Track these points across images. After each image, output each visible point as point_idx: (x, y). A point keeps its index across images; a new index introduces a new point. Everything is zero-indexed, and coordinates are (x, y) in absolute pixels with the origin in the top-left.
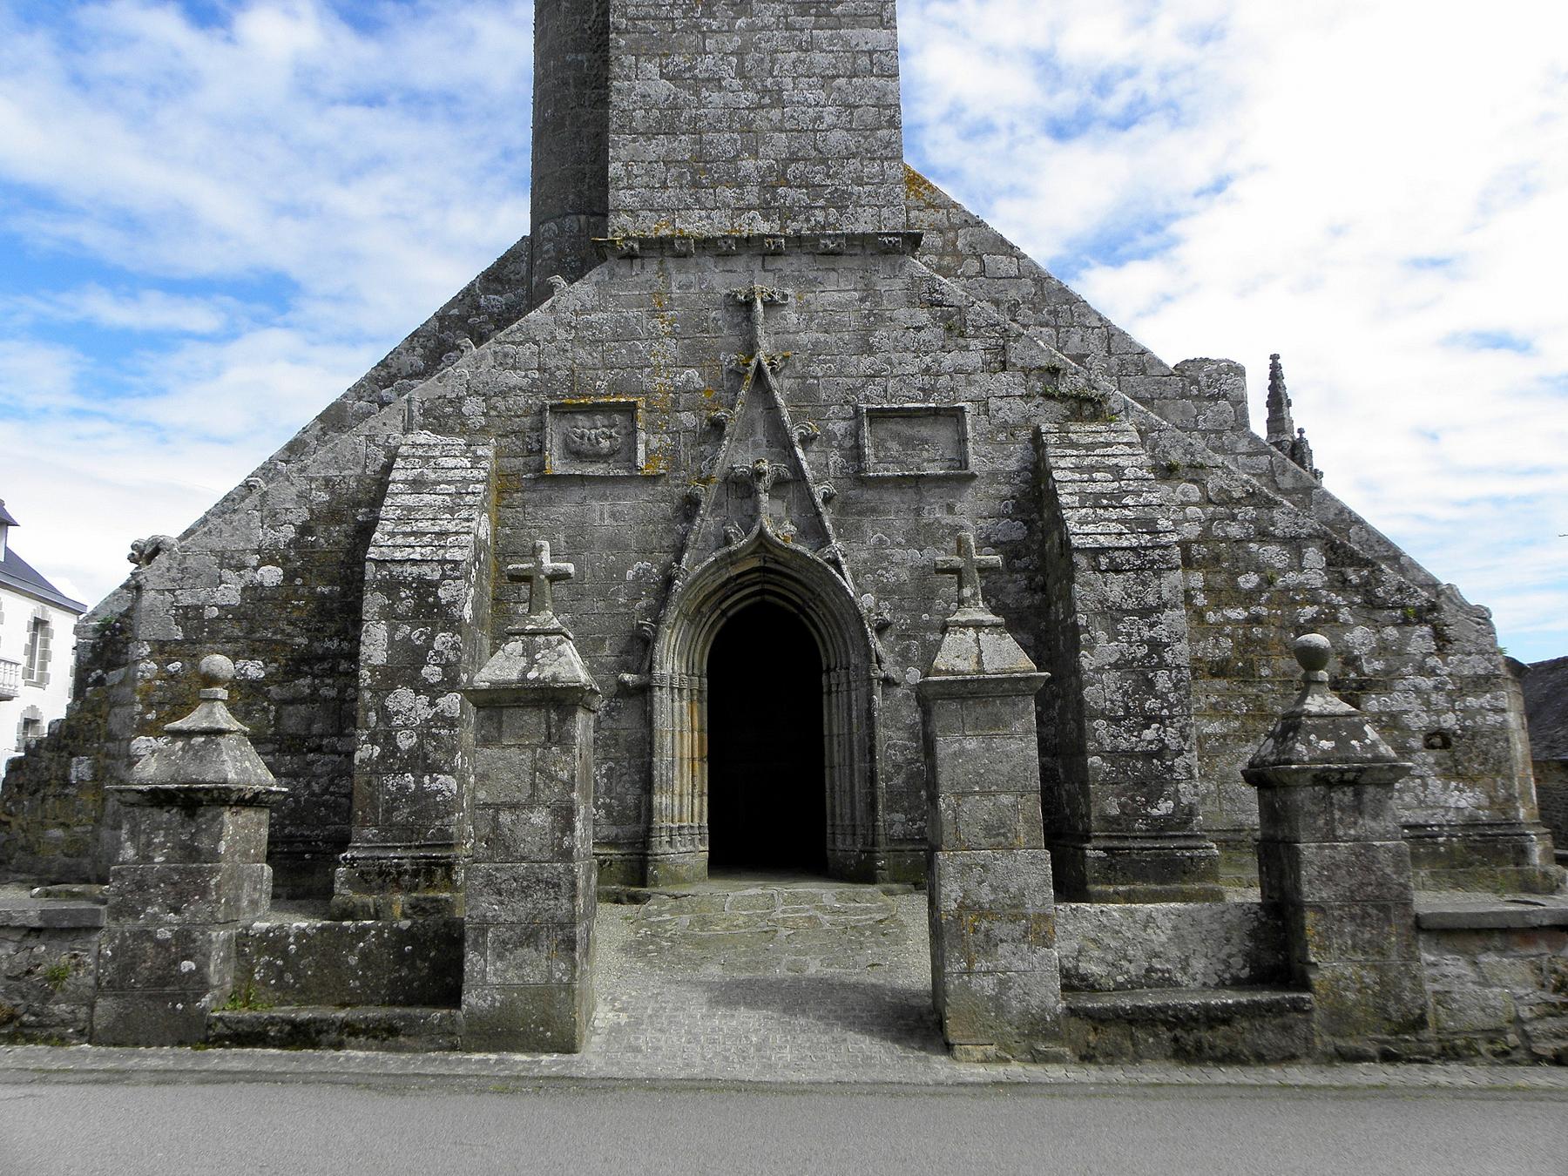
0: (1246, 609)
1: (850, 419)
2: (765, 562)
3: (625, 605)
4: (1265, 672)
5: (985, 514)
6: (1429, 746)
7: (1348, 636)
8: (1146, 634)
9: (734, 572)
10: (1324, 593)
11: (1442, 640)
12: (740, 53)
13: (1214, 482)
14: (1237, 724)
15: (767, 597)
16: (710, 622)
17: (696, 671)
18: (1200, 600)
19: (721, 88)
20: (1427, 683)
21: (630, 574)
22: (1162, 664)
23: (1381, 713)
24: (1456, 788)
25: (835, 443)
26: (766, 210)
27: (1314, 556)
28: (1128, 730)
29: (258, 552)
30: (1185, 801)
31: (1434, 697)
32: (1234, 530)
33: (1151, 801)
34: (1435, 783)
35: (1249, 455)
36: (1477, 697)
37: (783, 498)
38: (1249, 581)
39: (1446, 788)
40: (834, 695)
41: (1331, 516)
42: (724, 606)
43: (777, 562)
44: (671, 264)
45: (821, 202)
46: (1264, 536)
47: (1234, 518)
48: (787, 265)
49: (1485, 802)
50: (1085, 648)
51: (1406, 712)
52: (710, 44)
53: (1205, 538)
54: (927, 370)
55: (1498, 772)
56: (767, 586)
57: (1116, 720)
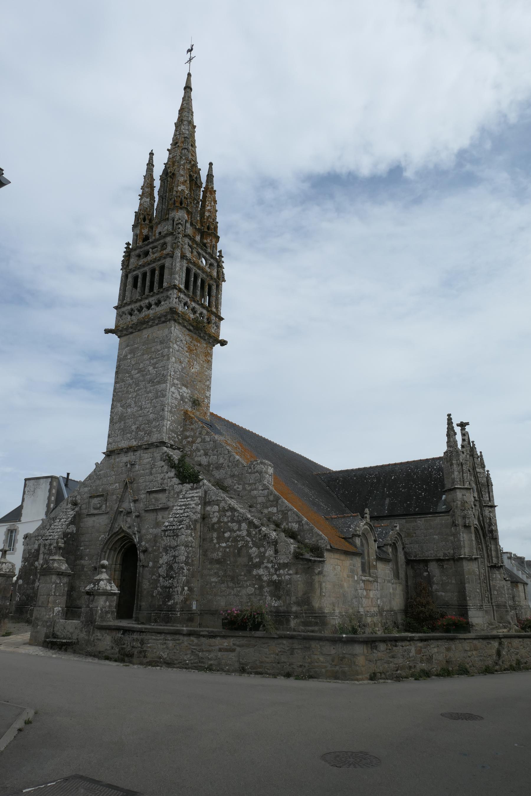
0: (226, 543)
4: (229, 562)
6: (268, 586)
7: (250, 551)
8: (174, 553)
9: (119, 537)
10: (246, 537)
11: (276, 552)
12: (135, 397)
13: (222, 504)
14: (220, 578)
18: (215, 541)
19: (131, 407)
20: (270, 565)
22: (175, 562)
23: (256, 575)
24: (275, 600)
26: (136, 439)
27: (244, 525)
28: (167, 581)
29: (41, 536)
30: (176, 601)
31: (271, 570)
32: (226, 520)
33: (169, 601)
34: (269, 598)
35: (262, 490)
36: (283, 570)
37: (130, 517)
38: (227, 535)
39: (271, 599)
41: (283, 509)
44: (116, 456)
45: (146, 435)
46: (233, 521)
47: (225, 515)
48: (138, 453)
49: (282, 604)
50: (160, 558)
51: (263, 575)
52: (130, 396)
53: (219, 522)
54: (162, 479)
55: (287, 595)
57: (164, 578)
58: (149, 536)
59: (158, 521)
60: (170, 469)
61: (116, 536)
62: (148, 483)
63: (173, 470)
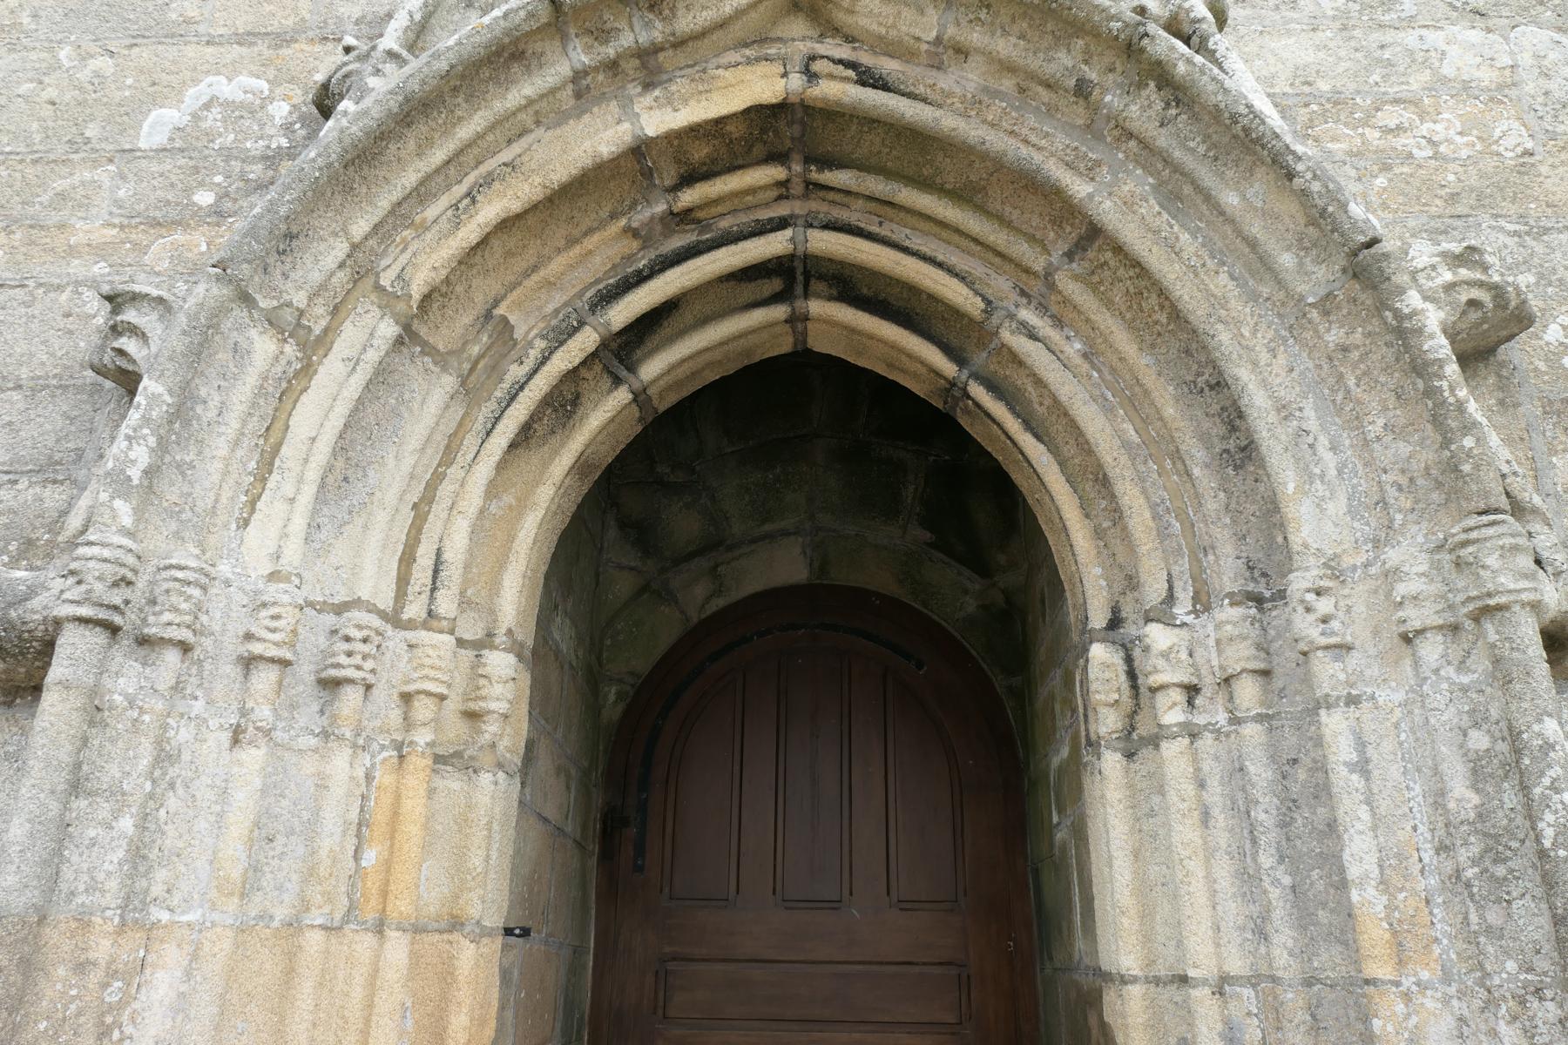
2: (812, 76)
3: (100, 251)
15: (822, 309)
16: (540, 385)
17: (446, 604)
21: (157, 126)
40: (1173, 750)
42: (622, 313)
43: (868, 79)
56: (824, 243)
58: (1446, 126)
61: (583, 90)
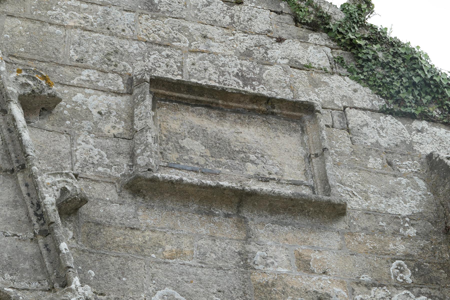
1: (117, 93)
5: (366, 278)
25: (87, 124)
59: (258, 278)
60: (293, 29)
62: (134, 48)
63: (313, 37)
